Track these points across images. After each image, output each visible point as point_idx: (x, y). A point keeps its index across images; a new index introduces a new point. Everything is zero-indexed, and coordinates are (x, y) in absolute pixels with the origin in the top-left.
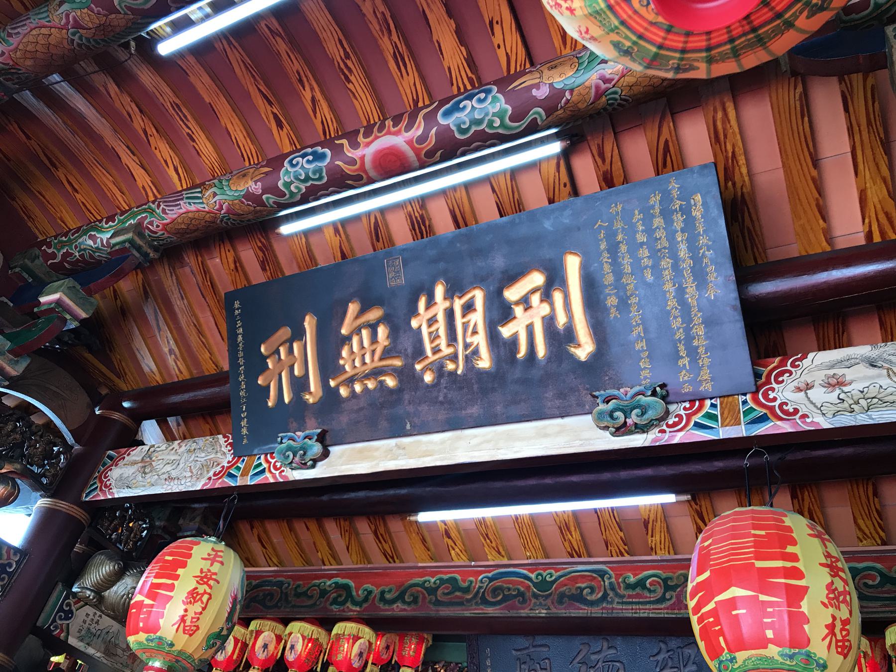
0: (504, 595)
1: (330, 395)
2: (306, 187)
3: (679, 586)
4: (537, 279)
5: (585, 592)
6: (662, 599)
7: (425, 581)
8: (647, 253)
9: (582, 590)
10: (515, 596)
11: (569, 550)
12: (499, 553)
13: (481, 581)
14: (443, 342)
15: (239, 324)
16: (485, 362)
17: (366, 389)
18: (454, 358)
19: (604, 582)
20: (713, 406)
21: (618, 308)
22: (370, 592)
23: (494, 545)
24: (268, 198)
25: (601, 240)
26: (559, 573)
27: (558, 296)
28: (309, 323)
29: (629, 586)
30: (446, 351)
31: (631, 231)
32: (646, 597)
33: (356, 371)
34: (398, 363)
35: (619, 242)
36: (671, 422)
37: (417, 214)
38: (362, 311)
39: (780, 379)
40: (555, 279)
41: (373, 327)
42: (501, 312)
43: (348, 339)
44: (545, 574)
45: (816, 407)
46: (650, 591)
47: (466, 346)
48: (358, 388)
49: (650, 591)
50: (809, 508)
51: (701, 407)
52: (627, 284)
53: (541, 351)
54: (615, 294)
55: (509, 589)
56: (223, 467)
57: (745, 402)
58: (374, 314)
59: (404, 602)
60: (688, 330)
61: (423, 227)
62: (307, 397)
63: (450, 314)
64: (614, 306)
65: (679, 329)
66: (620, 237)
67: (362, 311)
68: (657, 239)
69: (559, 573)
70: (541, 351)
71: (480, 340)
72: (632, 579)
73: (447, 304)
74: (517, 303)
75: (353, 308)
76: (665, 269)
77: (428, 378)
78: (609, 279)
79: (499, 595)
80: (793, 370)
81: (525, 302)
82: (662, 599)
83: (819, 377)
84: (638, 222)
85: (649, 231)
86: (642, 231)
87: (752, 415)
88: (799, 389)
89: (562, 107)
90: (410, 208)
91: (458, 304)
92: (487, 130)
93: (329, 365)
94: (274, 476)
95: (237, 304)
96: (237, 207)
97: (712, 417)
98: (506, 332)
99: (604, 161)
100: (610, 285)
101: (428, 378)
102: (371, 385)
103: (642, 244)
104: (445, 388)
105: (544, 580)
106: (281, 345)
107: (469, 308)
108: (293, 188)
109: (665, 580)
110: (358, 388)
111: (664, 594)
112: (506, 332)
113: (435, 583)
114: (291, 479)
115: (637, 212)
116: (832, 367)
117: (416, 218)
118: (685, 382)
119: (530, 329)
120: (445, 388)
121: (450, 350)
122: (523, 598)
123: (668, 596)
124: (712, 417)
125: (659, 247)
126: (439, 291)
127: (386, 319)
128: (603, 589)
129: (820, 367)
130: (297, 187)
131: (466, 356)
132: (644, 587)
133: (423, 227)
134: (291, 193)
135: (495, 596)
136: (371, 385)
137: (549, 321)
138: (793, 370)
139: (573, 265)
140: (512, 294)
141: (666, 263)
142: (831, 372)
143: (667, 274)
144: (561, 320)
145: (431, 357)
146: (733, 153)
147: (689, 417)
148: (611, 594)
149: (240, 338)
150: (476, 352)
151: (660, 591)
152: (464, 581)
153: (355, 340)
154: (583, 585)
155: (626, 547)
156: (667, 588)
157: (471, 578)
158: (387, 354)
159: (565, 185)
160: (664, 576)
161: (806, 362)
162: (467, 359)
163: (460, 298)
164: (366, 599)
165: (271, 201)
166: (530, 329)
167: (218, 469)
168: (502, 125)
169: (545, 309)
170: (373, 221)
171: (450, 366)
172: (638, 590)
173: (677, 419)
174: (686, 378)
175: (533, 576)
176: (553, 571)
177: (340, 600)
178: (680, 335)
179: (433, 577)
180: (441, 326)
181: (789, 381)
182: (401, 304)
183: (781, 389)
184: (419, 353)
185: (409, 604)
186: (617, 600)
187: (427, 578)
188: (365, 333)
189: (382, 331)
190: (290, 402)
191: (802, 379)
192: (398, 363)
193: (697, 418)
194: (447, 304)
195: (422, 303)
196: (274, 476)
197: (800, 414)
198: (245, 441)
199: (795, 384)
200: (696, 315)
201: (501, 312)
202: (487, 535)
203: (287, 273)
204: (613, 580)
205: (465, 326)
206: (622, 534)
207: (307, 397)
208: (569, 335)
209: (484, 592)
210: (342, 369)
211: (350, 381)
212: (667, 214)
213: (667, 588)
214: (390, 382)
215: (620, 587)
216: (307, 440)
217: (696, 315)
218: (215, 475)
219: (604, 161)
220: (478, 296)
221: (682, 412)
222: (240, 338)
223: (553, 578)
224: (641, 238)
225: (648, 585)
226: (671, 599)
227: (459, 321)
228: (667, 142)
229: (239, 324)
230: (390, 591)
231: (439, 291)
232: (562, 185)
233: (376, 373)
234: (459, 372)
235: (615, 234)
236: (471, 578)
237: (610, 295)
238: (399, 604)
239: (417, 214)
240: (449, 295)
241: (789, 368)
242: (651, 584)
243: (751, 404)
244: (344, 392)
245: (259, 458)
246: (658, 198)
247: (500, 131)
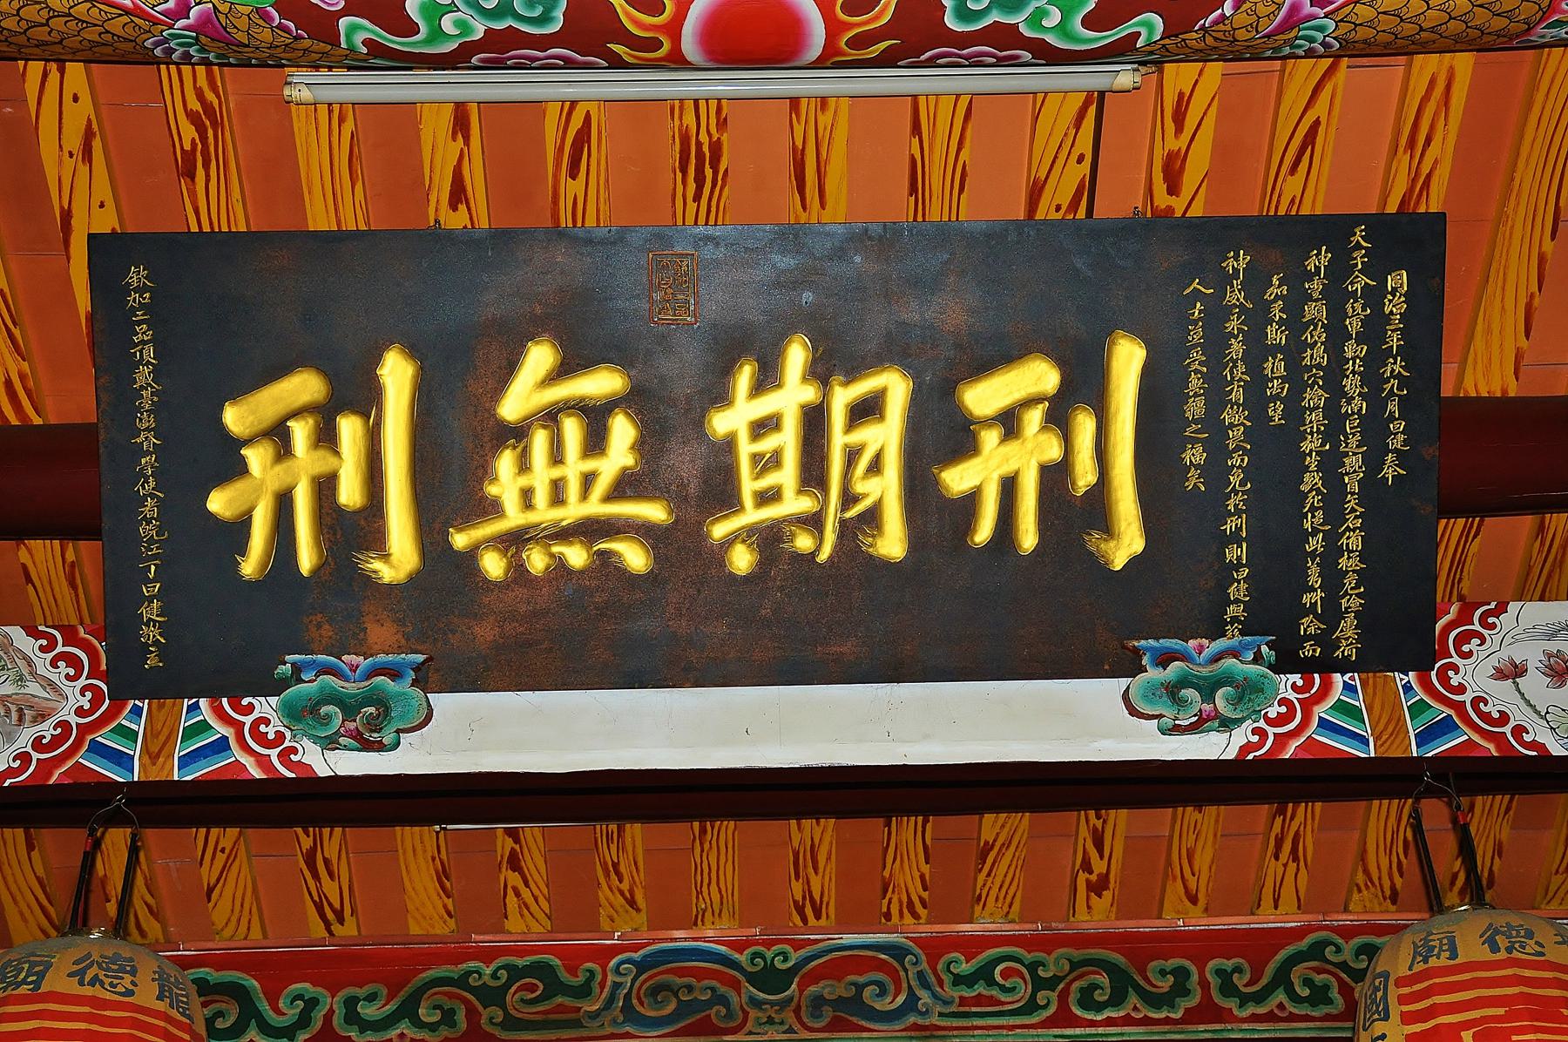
0: (679, 1000)
1: (444, 570)
2: (488, 31)
3: (1061, 979)
4: (1039, 376)
5: (868, 993)
6: (1031, 1007)
7: (469, 973)
8: (1281, 369)
9: (860, 988)
10: (709, 1004)
11: (799, 897)
12: (632, 902)
13: (617, 971)
14: (787, 476)
15: (143, 333)
16: (892, 543)
17: (560, 564)
18: (814, 522)
19: (906, 971)
20: (1348, 687)
21: (1203, 469)
22: (312, 1003)
23: (625, 886)
24: (353, 29)
25: (1195, 323)
26: (803, 953)
27: (1085, 426)
28: (397, 374)
29: (958, 980)
30: (795, 504)
31: (1257, 318)
32: (1003, 1003)
33: (532, 517)
34: (654, 512)
35: (1231, 335)
36: (1272, 714)
37: (704, 138)
38: (564, 370)
39: (1465, 648)
40: (1085, 385)
41: (595, 417)
42: (941, 434)
43: (518, 434)
44: (769, 955)
45: (1538, 713)
46: (1003, 989)
47: (849, 498)
48: (537, 561)
49: (1003, 989)
50: (1297, 834)
51: (1326, 688)
52: (1232, 426)
53: (1028, 539)
54: (1204, 442)
55: (690, 988)
56: (65, 725)
57: (1408, 688)
58: (602, 383)
59: (418, 1024)
60: (1332, 539)
61: (709, 172)
62: (377, 565)
63: (814, 420)
64: (1197, 467)
65: (1315, 532)
66: (1233, 325)
67: (564, 370)
68: (1307, 345)
69: (803, 953)
70: (1028, 539)
71: (885, 489)
72: (964, 968)
73: (810, 394)
74: (988, 422)
75: (540, 357)
76: (1312, 410)
77: (742, 560)
78: (1196, 408)
79: (665, 1002)
80: (1485, 632)
81: (1009, 422)
82: (1031, 1007)
83: (1532, 654)
84: (1275, 301)
85: (1295, 324)
86: (1281, 322)
87: (1426, 719)
88: (1500, 674)
89: (1203, 28)
90: (690, 119)
91: (842, 397)
92: (1023, 29)
93: (449, 485)
94: (263, 761)
95: (136, 276)
96: (243, 23)
97: (1353, 712)
98: (957, 479)
99: (1179, 128)
100: (1195, 421)
101: (742, 560)
102: (576, 556)
103: (1275, 349)
104: (781, 589)
105: (770, 968)
106: (296, 414)
107: (866, 410)
108: (447, 24)
109: (1033, 967)
110: (537, 561)
111: (1033, 997)
112: (957, 479)
113: (494, 976)
114: (322, 771)
115: (1275, 280)
116: (1551, 636)
117: (699, 144)
118: (1308, 638)
119: (1009, 486)
120: (781, 589)
121: (805, 504)
122: (728, 1009)
123: (1041, 998)
124: (1353, 712)
125: (1307, 361)
126: (796, 356)
127: (633, 401)
128: (905, 985)
129: (1533, 634)
130: (459, 24)
131: (843, 523)
132: (991, 982)
133: (709, 172)
134: (437, 34)
135: (659, 1004)
136: (576, 556)
137: (1055, 476)
138: (1485, 632)
139: (1128, 360)
140: (984, 397)
141: (1315, 397)
142: (1553, 646)
143: (1315, 419)
144: (1085, 475)
145: (752, 515)
146: (1429, 176)
147: (1307, 705)
148: (925, 997)
149: (143, 375)
150: (872, 517)
151: (1023, 991)
152: (573, 971)
153: (540, 440)
154: (861, 979)
155: (925, 895)
156: (1039, 984)
157: (589, 965)
158: (624, 487)
159: (1080, 159)
160: (1029, 957)
161: (1506, 620)
162: (848, 530)
163: (846, 384)
164: (303, 1021)
165: (358, 38)
166: (1009, 486)
167: (47, 730)
168: (1061, 28)
169: (1052, 450)
170: (577, 122)
171: (804, 542)
172: (980, 988)
173: (1283, 709)
174: (1312, 630)
175: (742, 958)
176: (788, 948)
177: (220, 1024)
178: (1315, 544)
179: (488, 963)
180: (788, 439)
181: (1482, 655)
182: (681, 367)
183: (1470, 669)
184: (724, 497)
185: (432, 1027)
186: (938, 1009)
187: (472, 965)
188: (572, 429)
189: (622, 431)
190: (316, 571)
191: (1504, 654)
192: (654, 512)
193: (1321, 711)
194: (810, 394)
195: (745, 376)
196: (263, 761)
197: (1512, 724)
198: (152, 661)
199: (1494, 661)
200: (1353, 510)
201: (941, 434)
202: (616, 866)
203: (319, 219)
204: (924, 966)
205: (852, 455)
206: (926, 869)
207: (377, 565)
208: (1096, 509)
209: (628, 997)
210: (494, 508)
211: (514, 541)
212: (1336, 298)
213: (1039, 984)
214: (634, 557)
215: (941, 983)
216: (380, 679)
217: (1353, 510)
218: (38, 744)
219: (1179, 128)
220: (896, 387)
221: (1292, 696)
222: (143, 375)
223: (790, 964)
224: (1275, 335)
225: (998, 978)
226: (1045, 1007)
227: (838, 439)
228: (1317, 122)
229: (143, 333)
230: (371, 998)
231: (796, 356)
232: (1074, 157)
233: (589, 530)
234: (823, 556)
235: (1226, 313)
236: (589, 965)
237: (1194, 441)
238: (404, 1027)
239: (704, 138)
240: (820, 372)
241: (1477, 627)
242: (1004, 974)
243: (1421, 694)
244: (493, 565)
245: (194, 708)
246: (1324, 261)
247: (1051, 39)
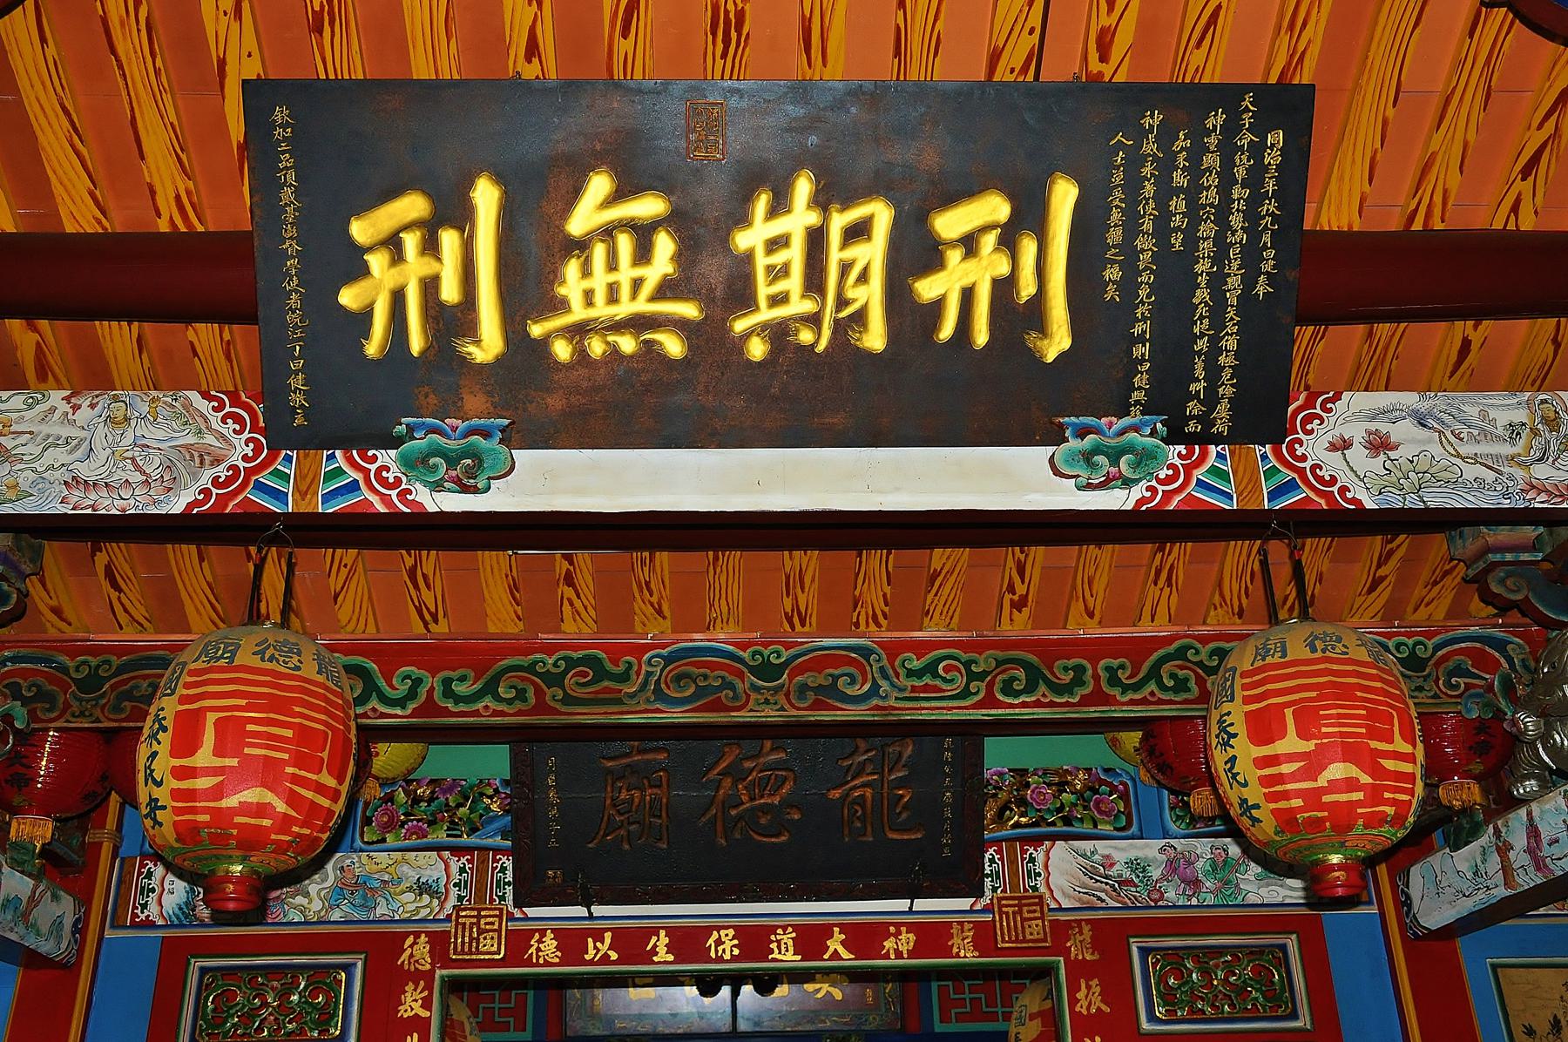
1: (524, 353)
3: (989, 673)
4: (996, 208)
5: (840, 682)
6: (965, 693)
8: (1182, 206)
9: (836, 678)
10: (720, 688)
12: (660, 612)
13: (649, 662)
14: (794, 283)
15: (286, 161)
16: (875, 338)
17: (614, 352)
18: (814, 320)
20: (1220, 456)
23: (654, 599)
26: (792, 651)
28: (486, 197)
29: (911, 673)
30: (801, 305)
31: (1166, 165)
33: (591, 313)
34: (689, 310)
36: (1162, 476)
38: (619, 195)
39: (1309, 427)
40: (1029, 216)
41: (643, 234)
42: (915, 252)
43: (581, 246)
44: (766, 652)
46: (945, 680)
47: (842, 302)
48: (596, 347)
49: (945, 680)
52: (1143, 251)
53: (981, 337)
55: (706, 677)
56: (234, 468)
58: (649, 206)
59: (498, 699)
60: (1214, 341)
61: (734, 35)
62: (471, 349)
63: (816, 239)
65: (1202, 335)
66: (1147, 170)
67: (619, 195)
69: (792, 651)
70: (981, 337)
71: (871, 295)
72: (915, 664)
73: (813, 218)
74: (952, 244)
75: (599, 185)
77: (757, 349)
78: (1115, 236)
81: (969, 244)
82: (965, 693)
83: (1357, 432)
85: (1195, 171)
87: (1277, 480)
88: (1333, 447)
91: (839, 221)
93: (528, 287)
94: (386, 500)
95: (280, 114)
97: (1222, 475)
98: (927, 288)
100: (1114, 246)
101: (757, 349)
102: (627, 344)
103: (1180, 190)
104: (787, 372)
105: (766, 663)
106: (407, 227)
107: (858, 232)
109: (967, 665)
110: (596, 347)
111: (968, 685)
112: (927, 288)
113: (555, 665)
114: (431, 508)
115: (1181, 136)
116: (1373, 418)
117: (727, 12)
118: (1192, 417)
119: (968, 295)
120: (787, 372)
121: (808, 306)
123: (973, 687)
124: (1222, 475)
125: (1203, 201)
126: (803, 187)
127: (675, 221)
129: (1359, 416)
131: (837, 322)
132: (936, 675)
133: (734, 35)
136: (627, 344)
137: (1004, 287)
139: (1064, 196)
140: (950, 224)
141: (1207, 229)
142: (1373, 426)
143: (1206, 247)
145: (765, 314)
146: (1303, 53)
147: (1188, 470)
149: (287, 194)
150: (860, 317)
152: (616, 663)
153: (599, 251)
154: (836, 672)
156: (972, 677)
158: (666, 290)
159: (1031, 32)
160: (965, 657)
164: (412, 694)
166: (968, 295)
167: (222, 472)
169: (1003, 268)
171: (806, 336)
172: (927, 680)
173: (1170, 472)
174: (1195, 412)
175: (746, 655)
178: (1202, 345)
180: (795, 255)
182: (712, 192)
184: (743, 298)
185: (509, 702)
188: (625, 243)
189: (664, 245)
190: (423, 353)
192: (689, 310)
193: (1198, 474)
194: (813, 218)
195: (762, 203)
196: (386, 500)
197: (1339, 484)
199: (1329, 437)
201: (915, 252)
202: (647, 584)
203: (421, 70)
204: (885, 662)
205: (845, 268)
206: (888, 590)
207: (471, 349)
210: (562, 305)
211: (579, 332)
212: (1228, 151)
213: (972, 677)
214: (673, 346)
220: (881, 214)
221: (1177, 462)
222: (287, 194)
225: (941, 672)
227: (835, 255)
229: (286, 161)
230: (462, 679)
231: (803, 187)
233: (638, 324)
234: (821, 348)
237: (1113, 262)
238: (488, 701)
240: (822, 201)
241: (1318, 411)
242: (946, 669)
244: (562, 350)
245: (332, 457)
246: (1220, 121)
